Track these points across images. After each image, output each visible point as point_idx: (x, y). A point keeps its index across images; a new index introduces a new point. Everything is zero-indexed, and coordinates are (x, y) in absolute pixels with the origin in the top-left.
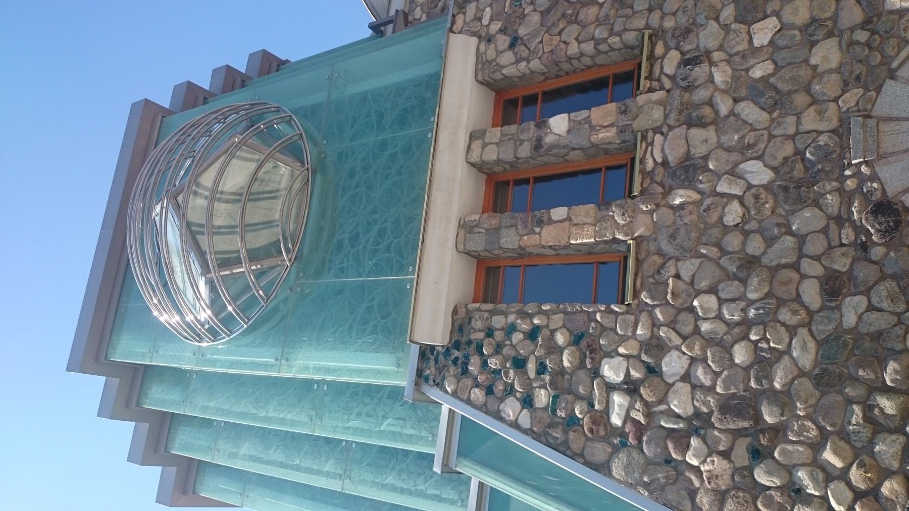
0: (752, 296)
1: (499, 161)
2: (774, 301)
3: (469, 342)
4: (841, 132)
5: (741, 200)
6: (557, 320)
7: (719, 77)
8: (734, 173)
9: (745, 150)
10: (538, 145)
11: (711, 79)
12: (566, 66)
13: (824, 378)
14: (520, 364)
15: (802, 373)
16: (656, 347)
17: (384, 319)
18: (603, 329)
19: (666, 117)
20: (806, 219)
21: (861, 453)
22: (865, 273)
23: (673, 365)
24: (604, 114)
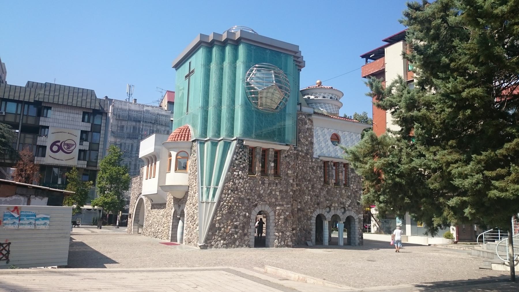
4: (265, 201)
7: (274, 188)
8: (262, 189)
9: (264, 190)
10: (270, 161)
13: (240, 198)
14: (241, 158)
16: (243, 179)
17: (247, 131)
20: (256, 197)
21: (233, 201)
23: (241, 181)
24: (272, 172)
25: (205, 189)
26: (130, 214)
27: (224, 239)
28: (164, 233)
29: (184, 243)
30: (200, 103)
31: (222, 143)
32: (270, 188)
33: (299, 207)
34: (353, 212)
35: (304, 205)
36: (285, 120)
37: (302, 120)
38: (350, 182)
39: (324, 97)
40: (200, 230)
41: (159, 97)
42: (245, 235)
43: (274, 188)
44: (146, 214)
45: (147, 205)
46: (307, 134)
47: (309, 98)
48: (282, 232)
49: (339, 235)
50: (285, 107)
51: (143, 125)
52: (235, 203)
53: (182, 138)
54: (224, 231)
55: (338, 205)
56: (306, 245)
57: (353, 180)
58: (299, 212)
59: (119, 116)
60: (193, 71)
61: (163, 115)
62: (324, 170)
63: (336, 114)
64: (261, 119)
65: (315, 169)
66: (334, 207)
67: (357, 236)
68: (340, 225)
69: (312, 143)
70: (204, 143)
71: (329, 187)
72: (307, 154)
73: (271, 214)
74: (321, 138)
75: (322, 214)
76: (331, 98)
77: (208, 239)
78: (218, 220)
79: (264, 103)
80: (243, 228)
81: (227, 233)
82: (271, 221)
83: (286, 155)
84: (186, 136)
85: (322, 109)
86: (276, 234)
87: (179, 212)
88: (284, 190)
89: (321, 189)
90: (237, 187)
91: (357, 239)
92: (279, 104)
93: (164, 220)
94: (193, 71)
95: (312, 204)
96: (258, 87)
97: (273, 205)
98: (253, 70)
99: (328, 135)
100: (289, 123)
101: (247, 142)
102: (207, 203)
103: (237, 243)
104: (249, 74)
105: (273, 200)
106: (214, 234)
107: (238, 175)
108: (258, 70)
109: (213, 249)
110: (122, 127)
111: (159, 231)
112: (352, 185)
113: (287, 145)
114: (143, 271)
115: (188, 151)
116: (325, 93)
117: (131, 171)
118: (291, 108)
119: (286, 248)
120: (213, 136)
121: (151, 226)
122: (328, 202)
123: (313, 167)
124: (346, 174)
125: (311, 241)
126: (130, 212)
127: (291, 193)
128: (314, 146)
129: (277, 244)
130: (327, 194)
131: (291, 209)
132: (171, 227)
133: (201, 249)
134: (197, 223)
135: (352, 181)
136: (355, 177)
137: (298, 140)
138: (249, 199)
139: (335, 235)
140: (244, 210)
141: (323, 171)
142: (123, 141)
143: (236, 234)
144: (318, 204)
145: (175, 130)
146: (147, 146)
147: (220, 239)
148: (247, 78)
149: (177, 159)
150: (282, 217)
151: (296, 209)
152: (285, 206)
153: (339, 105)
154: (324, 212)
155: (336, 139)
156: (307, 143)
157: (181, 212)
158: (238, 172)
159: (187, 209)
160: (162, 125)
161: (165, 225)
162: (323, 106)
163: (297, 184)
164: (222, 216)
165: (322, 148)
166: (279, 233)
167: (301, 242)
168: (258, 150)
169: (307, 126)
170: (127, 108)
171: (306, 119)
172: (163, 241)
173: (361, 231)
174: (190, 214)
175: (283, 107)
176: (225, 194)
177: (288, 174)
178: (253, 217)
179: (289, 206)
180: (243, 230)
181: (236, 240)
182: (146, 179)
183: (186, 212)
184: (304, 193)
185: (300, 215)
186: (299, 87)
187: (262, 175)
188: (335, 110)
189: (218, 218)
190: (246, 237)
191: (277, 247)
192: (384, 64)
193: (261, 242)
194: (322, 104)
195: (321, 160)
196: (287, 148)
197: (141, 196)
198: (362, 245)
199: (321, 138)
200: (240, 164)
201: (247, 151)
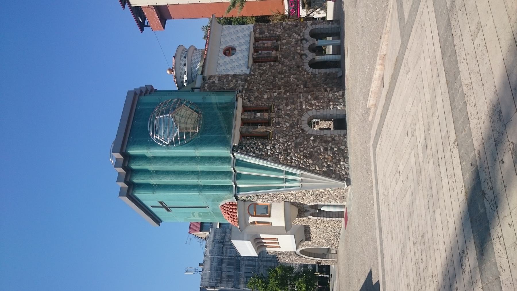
2: (290, 139)
4: (298, 121)
6: (259, 142)
7: (283, 112)
8: (285, 124)
9: (286, 122)
10: (255, 117)
13: (295, 147)
14: (253, 148)
16: (275, 144)
17: (224, 142)
18: (266, 143)
20: (293, 130)
21: (299, 154)
22: (300, 136)
23: (277, 147)
25: (287, 184)
26: (317, 262)
27: (339, 161)
28: (335, 225)
29: (345, 203)
30: (195, 194)
31: (238, 169)
32: (283, 116)
33: (302, 86)
34: (306, 31)
35: (301, 82)
36: (211, 104)
37: (210, 87)
38: (274, 35)
39: (185, 65)
40: (330, 187)
41: (196, 241)
42: (333, 139)
43: (283, 112)
44: (316, 246)
45: (307, 245)
46: (225, 80)
47: (186, 81)
48: (329, 101)
49: (330, 45)
50: (196, 104)
51: (226, 256)
52: (301, 151)
53: (234, 211)
54: (331, 161)
55: (298, 46)
56: (342, 78)
57: (272, 32)
58: (307, 86)
59: (217, 280)
60: (161, 203)
61: (215, 236)
62: (262, 62)
63: (203, 52)
64: (210, 128)
65: (262, 72)
66: (301, 50)
67: (330, 25)
68: (319, 43)
69: (234, 76)
70: (239, 188)
71: (280, 56)
72: (246, 80)
73: (310, 113)
74: (229, 66)
75: (309, 63)
76: (185, 57)
77: (340, 178)
78: (319, 168)
79: (192, 126)
80: (327, 142)
81: (333, 159)
82: (318, 113)
84: (231, 207)
85: (198, 67)
86: (331, 107)
87: (313, 211)
88: (285, 101)
89: (282, 64)
90: (284, 150)
91: (333, 26)
92: (193, 110)
93: (321, 227)
94: (161, 203)
95: (298, 73)
96: (174, 132)
97: (302, 112)
98: (157, 139)
99: (225, 60)
100: (214, 99)
101: (235, 141)
102: (302, 181)
103: (343, 147)
104: (161, 142)
105: (296, 112)
106: (334, 172)
107: (271, 150)
108: (156, 133)
109: (349, 172)
110: (228, 276)
111: (333, 231)
112: (278, 33)
113: (237, 100)
114: (381, 239)
115: (248, 204)
116: (180, 64)
117: (273, 265)
118: (197, 98)
119: (346, 96)
120: (230, 179)
121: (328, 240)
122: (296, 57)
123: (259, 73)
124: (266, 40)
125: (337, 72)
126: (315, 263)
127: (288, 94)
128: (238, 73)
129: (342, 106)
130: (287, 58)
131: (304, 94)
132: (328, 219)
133: (350, 184)
134: (323, 191)
135: (273, 33)
136: (268, 31)
137: (232, 90)
138: (296, 138)
139: (329, 50)
140: (308, 142)
141: (263, 63)
142: (243, 275)
143: (333, 149)
144: (299, 67)
145: (227, 220)
146: (245, 248)
147: (339, 166)
148: (165, 144)
149: (256, 216)
151: (305, 89)
152: (302, 100)
153: (192, 49)
154: (307, 60)
155: (229, 51)
156: (234, 81)
157: (313, 208)
158: (268, 150)
159: (309, 202)
160: (224, 237)
161: (327, 225)
162: (195, 65)
163: (278, 89)
164: (315, 164)
165: (239, 65)
166: (331, 105)
167: (338, 82)
168: (244, 130)
169: (217, 82)
170: (208, 273)
171: (209, 83)
172: (343, 226)
173: (324, 22)
174: (315, 199)
175: (196, 106)
176: (292, 162)
177: (268, 99)
178: (315, 133)
179: (301, 95)
180: (329, 142)
181: (339, 149)
182: (280, 247)
183: (312, 204)
184: (288, 82)
185: (310, 86)
186: (174, 91)
187: (270, 125)
188: (198, 53)
189: (317, 169)
190: (335, 138)
191: (345, 106)
192: (149, 7)
193: (341, 123)
194: (192, 67)
195: (252, 65)
196: (240, 100)
197: (298, 252)
198: (339, 20)
199: (229, 66)
200: (260, 149)
201: (245, 141)
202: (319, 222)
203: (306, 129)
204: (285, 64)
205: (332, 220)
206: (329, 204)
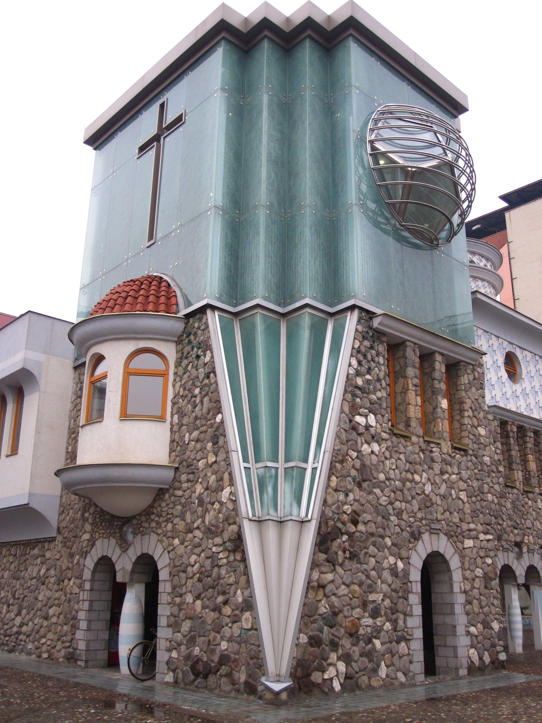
0: (397, 482)
1: (434, 369)
3: (374, 342)
5: (420, 482)
11: (454, 474)
12: (457, 407)
15: (378, 499)
19: (444, 454)
20: (415, 505)
23: (376, 447)
73: (454, 563)
83: (471, 377)
89: (502, 496)
94: (179, 121)
97: (455, 535)
107: (368, 427)
111: (24, 629)
122: (516, 531)
138: (399, 514)
149: (128, 373)
150: (479, 572)
158: (366, 416)
161: (51, 611)
180: (394, 623)
190: (403, 644)
202: (71, 584)
203: (420, 546)
204: (502, 501)
205: (75, 627)
206: (162, 621)
